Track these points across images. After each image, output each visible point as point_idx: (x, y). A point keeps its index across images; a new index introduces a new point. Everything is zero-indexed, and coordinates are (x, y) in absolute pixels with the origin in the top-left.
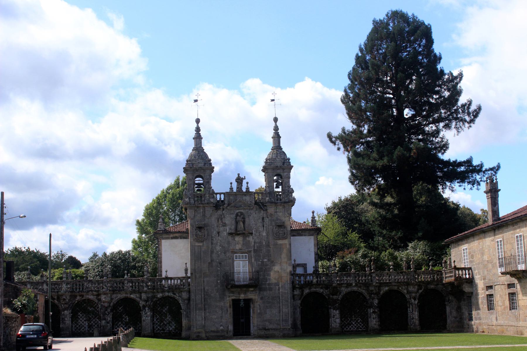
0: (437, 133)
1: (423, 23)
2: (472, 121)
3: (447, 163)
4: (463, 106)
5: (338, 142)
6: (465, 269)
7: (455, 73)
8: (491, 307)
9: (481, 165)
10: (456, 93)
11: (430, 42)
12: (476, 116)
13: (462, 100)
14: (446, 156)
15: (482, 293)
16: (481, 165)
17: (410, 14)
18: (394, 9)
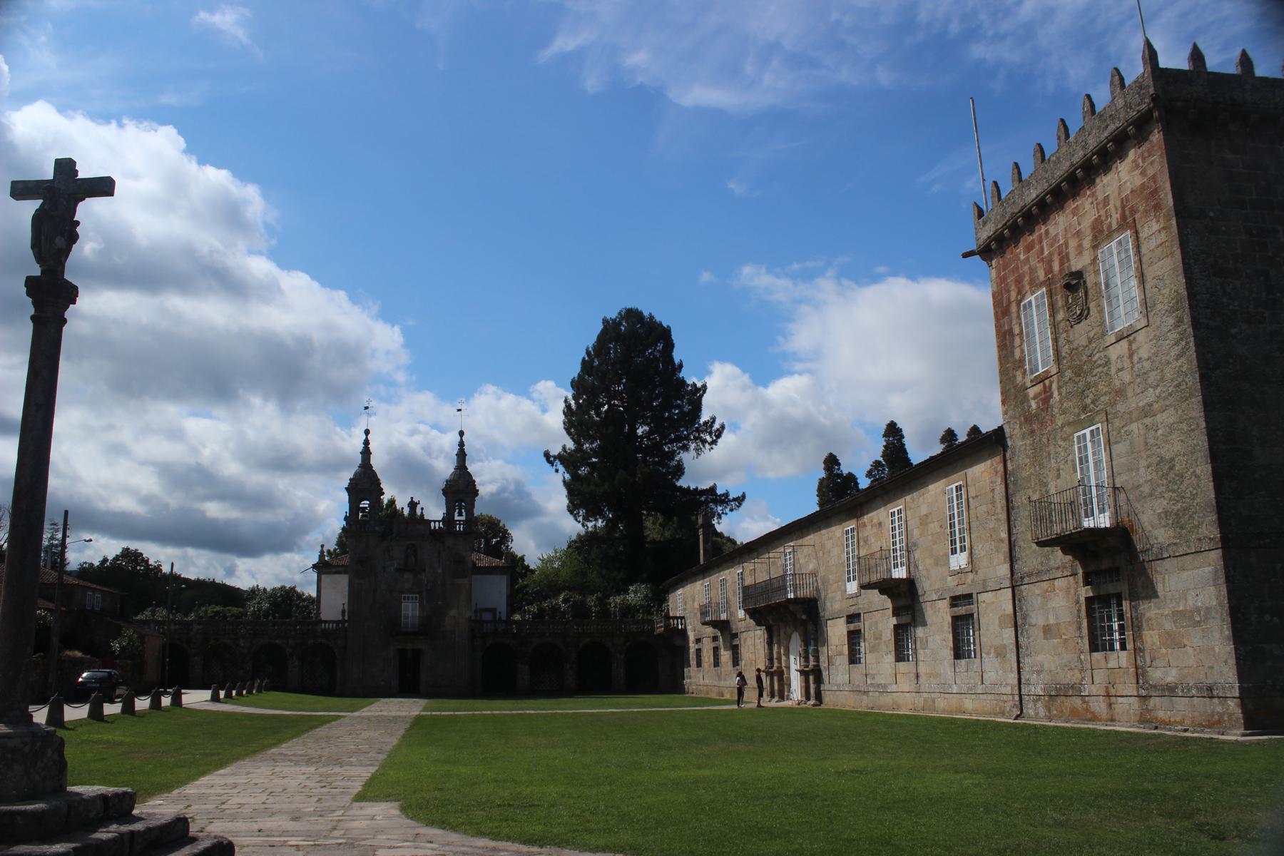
0: (672, 454)
1: (660, 324)
2: (714, 442)
3: (687, 491)
4: (706, 423)
5: (558, 462)
6: (677, 618)
7: (699, 385)
8: (699, 664)
9: (727, 494)
10: (697, 407)
11: (670, 345)
12: (719, 436)
13: (705, 417)
14: (683, 483)
15: (693, 647)
16: (727, 494)
17: (646, 314)
18: (629, 306)
